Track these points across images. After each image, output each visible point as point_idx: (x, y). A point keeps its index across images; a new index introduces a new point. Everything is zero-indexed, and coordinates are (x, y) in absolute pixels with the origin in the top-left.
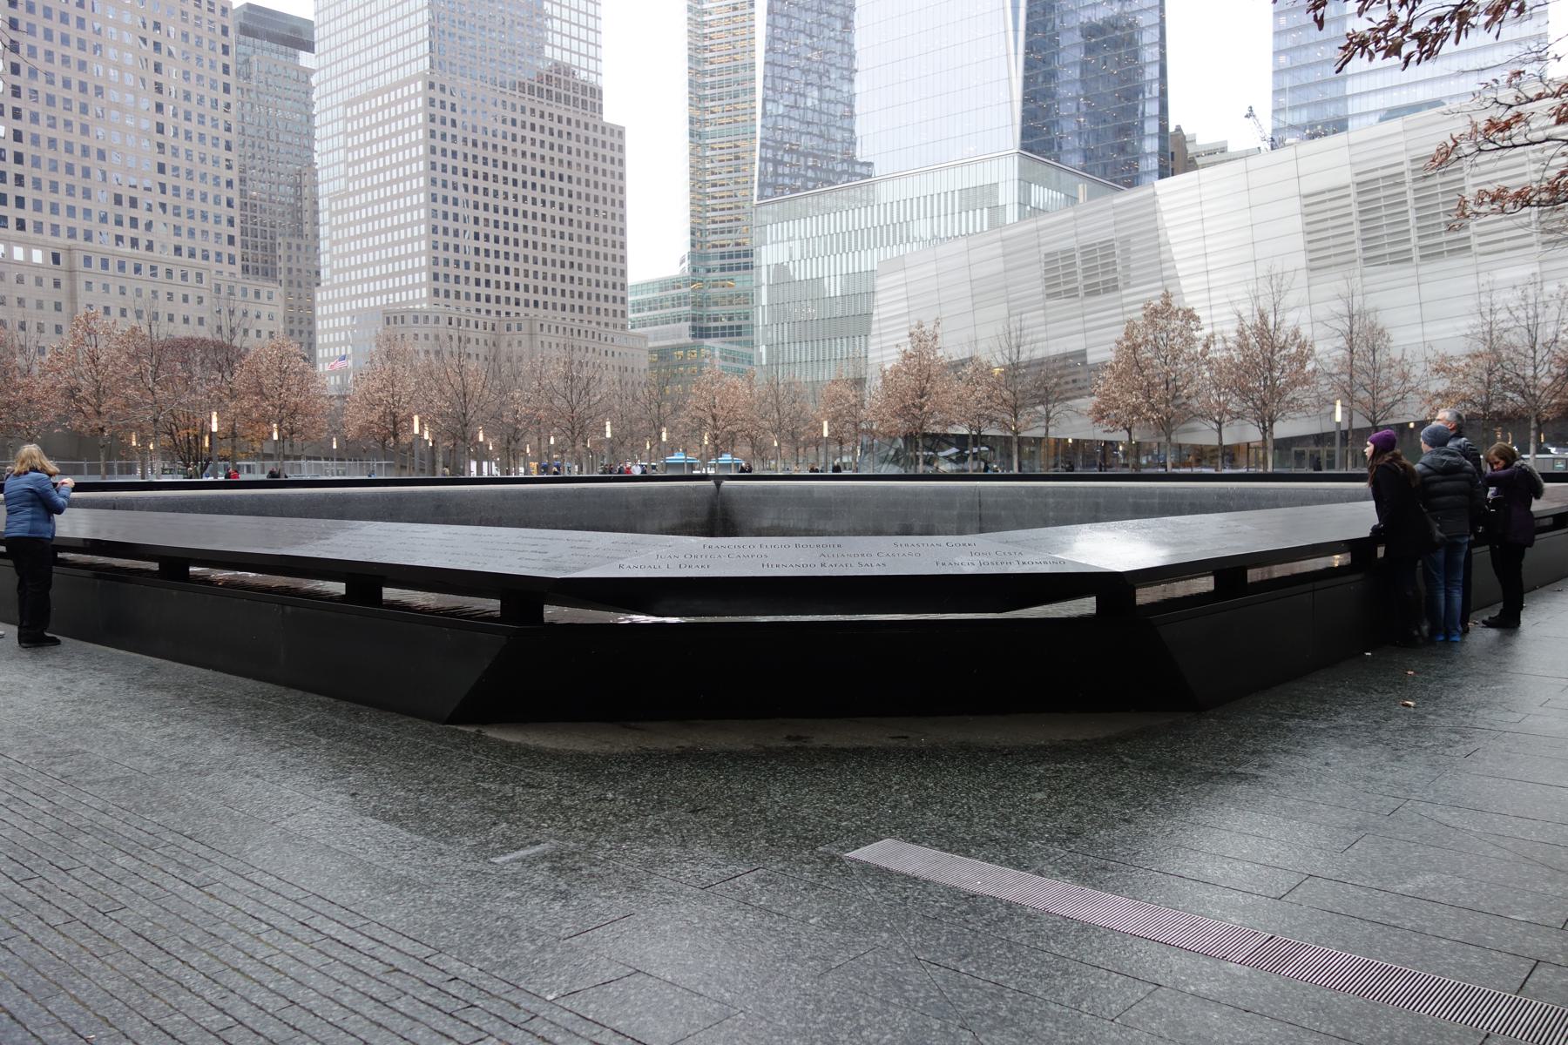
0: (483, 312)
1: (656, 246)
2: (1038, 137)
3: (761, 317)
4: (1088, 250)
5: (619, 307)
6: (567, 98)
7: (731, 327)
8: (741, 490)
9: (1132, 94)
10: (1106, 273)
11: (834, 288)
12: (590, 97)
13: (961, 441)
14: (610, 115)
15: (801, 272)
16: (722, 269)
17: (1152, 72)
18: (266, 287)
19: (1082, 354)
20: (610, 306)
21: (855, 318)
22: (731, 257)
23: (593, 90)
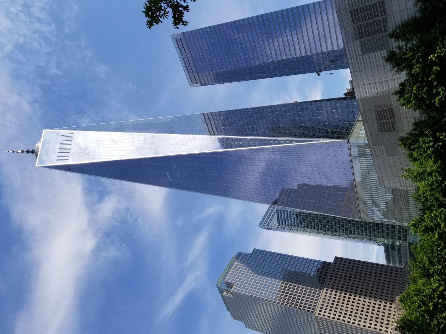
0: (394, 317)
5: (394, 269)
6: (325, 273)
7: (403, 232)
10: (386, 113)
11: (389, 197)
14: (331, 260)
16: (383, 232)
20: (394, 272)
22: (378, 229)
23: (324, 264)
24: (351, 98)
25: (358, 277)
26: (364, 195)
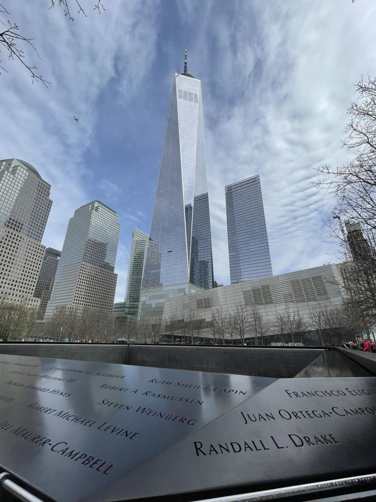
1: (120, 296)
2: (192, 281)
3: (140, 310)
4: (205, 299)
8: (133, 347)
9: (206, 273)
11: (154, 306)
12: (112, 269)
13: (180, 337)
15: (147, 303)
17: (210, 269)
18: (37, 299)
19: (204, 320)
21: (159, 311)
24: (213, 285)
25: (106, 287)
26: (154, 292)
